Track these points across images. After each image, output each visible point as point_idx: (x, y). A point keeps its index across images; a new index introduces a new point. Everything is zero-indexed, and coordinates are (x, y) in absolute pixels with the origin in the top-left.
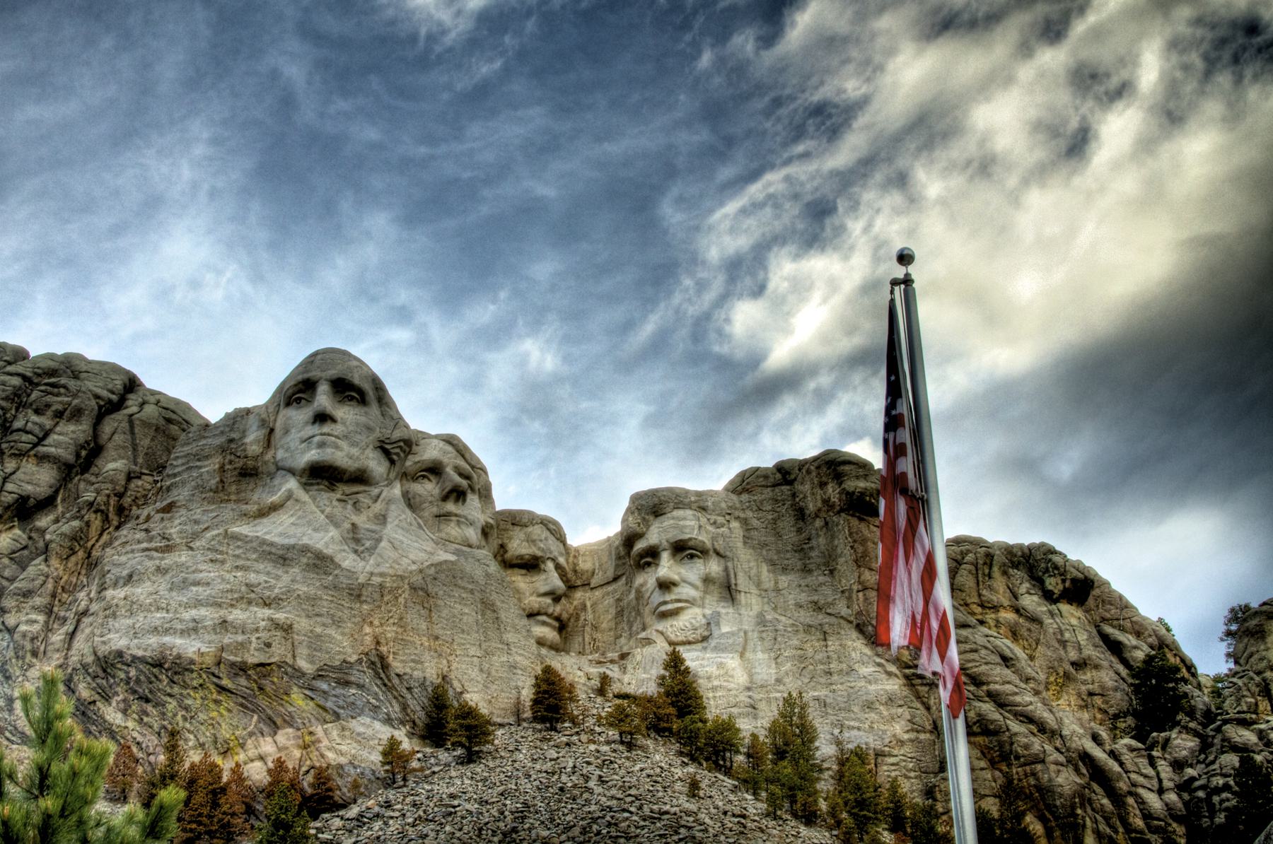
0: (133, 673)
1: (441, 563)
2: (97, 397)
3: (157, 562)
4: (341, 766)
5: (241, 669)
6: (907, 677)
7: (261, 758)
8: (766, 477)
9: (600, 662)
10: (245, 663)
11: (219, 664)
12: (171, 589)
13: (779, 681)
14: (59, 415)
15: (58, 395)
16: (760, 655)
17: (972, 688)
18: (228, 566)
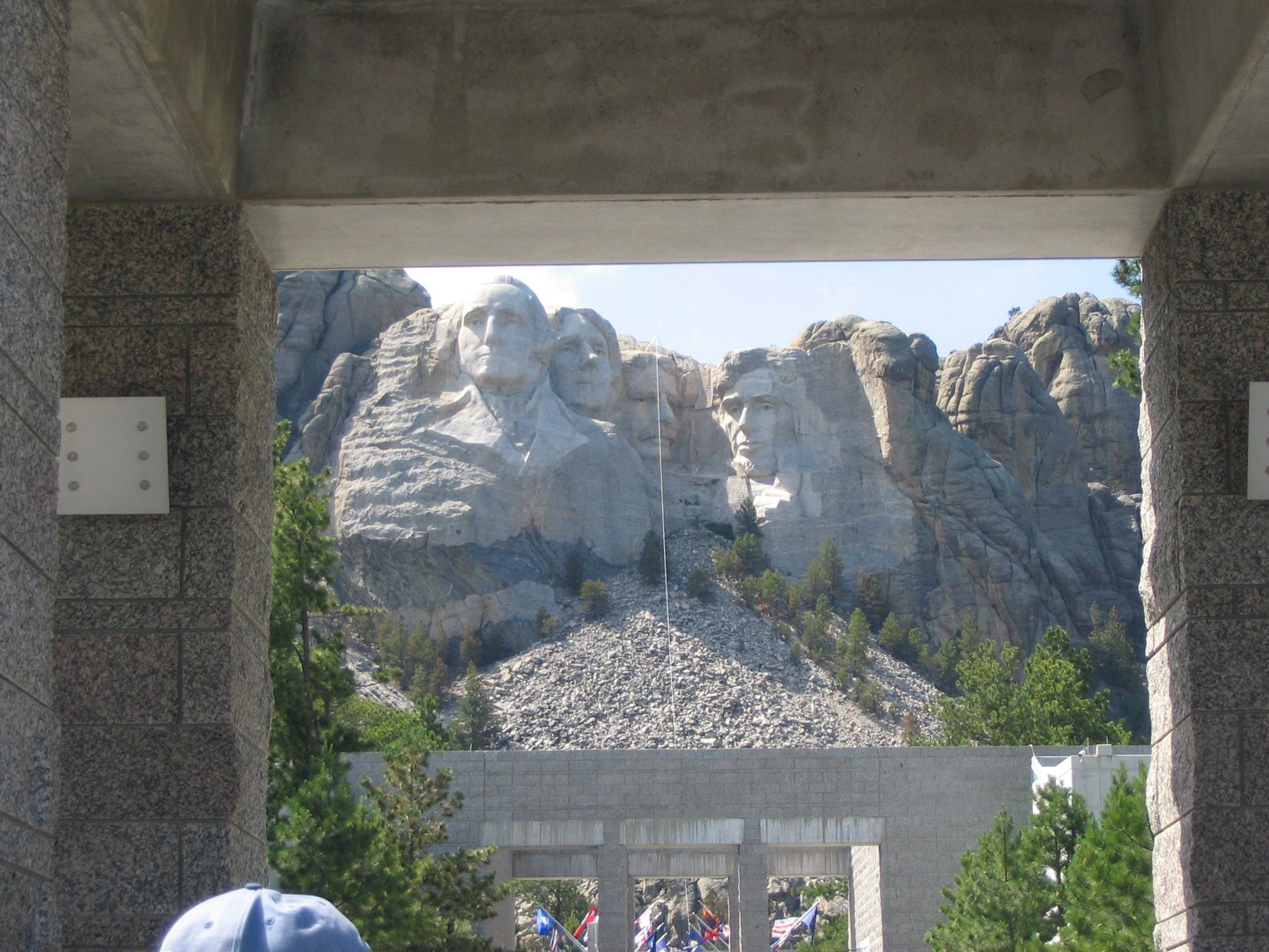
0: (368, 551)
1: (577, 449)
2: (323, 283)
3: (379, 459)
4: (509, 622)
5: (441, 551)
6: (917, 508)
7: (456, 615)
8: (828, 332)
9: (697, 485)
10: (443, 545)
11: (426, 545)
12: (390, 485)
13: (824, 515)
14: (298, 305)
15: (295, 288)
16: (811, 493)
17: (965, 520)
18: (428, 464)
